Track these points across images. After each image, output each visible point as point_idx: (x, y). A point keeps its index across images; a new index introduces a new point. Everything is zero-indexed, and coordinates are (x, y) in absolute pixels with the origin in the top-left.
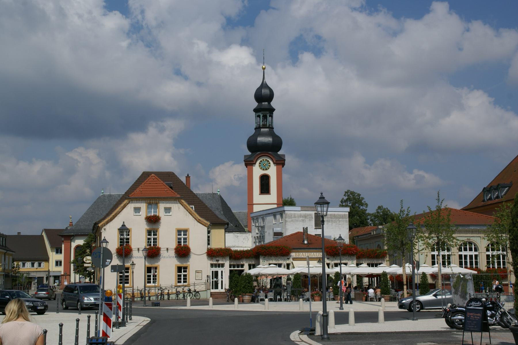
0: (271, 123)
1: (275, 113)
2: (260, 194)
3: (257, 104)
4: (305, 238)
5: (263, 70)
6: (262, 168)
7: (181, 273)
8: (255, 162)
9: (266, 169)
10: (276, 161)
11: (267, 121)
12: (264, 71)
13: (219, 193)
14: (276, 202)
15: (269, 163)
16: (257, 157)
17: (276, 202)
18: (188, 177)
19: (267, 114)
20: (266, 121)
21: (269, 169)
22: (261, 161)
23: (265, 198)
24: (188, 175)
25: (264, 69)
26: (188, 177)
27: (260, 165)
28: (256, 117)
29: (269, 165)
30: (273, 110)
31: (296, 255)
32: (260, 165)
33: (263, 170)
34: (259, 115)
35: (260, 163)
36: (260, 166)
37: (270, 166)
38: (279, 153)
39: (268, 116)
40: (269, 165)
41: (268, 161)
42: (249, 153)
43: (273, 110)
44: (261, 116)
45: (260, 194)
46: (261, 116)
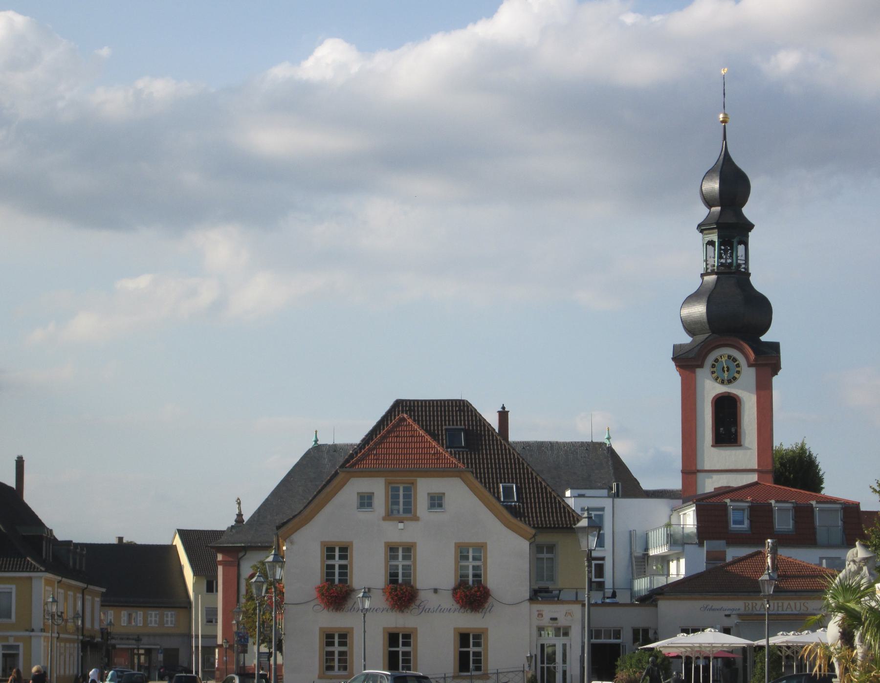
2: (713, 446)
6: (718, 377)
7: (398, 646)
8: (699, 363)
9: (730, 382)
14: (756, 467)
15: (738, 366)
17: (756, 467)
18: (503, 415)
22: (716, 360)
23: (727, 457)
24: (503, 408)
26: (503, 415)
28: (705, 245)
29: (738, 369)
30: (750, 227)
31: (747, 608)
32: (715, 369)
33: (723, 382)
34: (712, 241)
35: (713, 366)
36: (713, 373)
37: (738, 372)
38: (763, 338)
40: (738, 369)
41: (735, 360)
43: (750, 226)
45: (713, 446)
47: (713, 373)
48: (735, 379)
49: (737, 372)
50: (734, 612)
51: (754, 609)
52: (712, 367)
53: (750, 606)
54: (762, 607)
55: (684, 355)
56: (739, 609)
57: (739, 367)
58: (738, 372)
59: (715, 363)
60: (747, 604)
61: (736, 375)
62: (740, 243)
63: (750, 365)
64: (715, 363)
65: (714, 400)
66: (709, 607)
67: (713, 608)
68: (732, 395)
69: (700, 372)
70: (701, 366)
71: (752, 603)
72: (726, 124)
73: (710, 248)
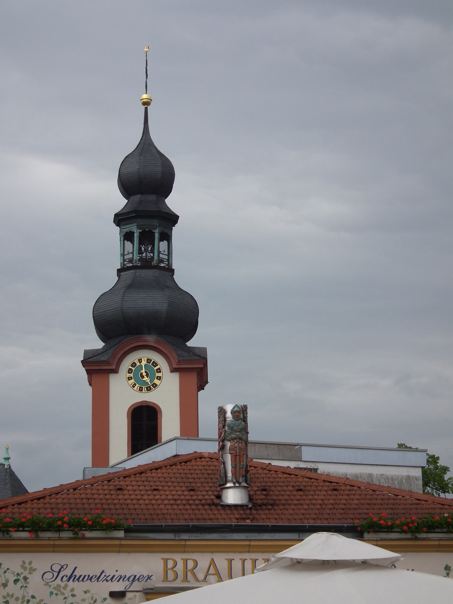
0: (166, 257)
1: (176, 231)
3: (127, 201)
4: (230, 474)
5: (143, 107)
6: (135, 384)
8: (113, 367)
9: (149, 389)
10: (179, 362)
11: (152, 251)
12: (146, 109)
13: (6, 463)
15: (159, 371)
16: (122, 352)
19: (155, 229)
20: (151, 250)
21: (158, 389)
22: (134, 365)
25: (146, 104)
27: (131, 375)
28: (122, 239)
29: (158, 375)
31: (171, 575)
32: (131, 375)
34: (130, 231)
35: (130, 371)
38: (190, 344)
39: (157, 236)
40: (158, 375)
41: (155, 364)
42: (99, 344)
44: (136, 235)
46: (136, 235)
47: (130, 378)
48: (155, 385)
49: (157, 378)
50: (137, 586)
51: (189, 573)
52: (129, 373)
53: (180, 566)
54: (212, 571)
55: (94, 358)
56: (149, 577)
57: (160, 372)
58: (159, 378)
59: (132, 368)
60: (170, 564)
61: (156, 381)
62: (161, 239)
63: (173, 370)
64: (132, 368)
65: (130, 413)
66: (68, 572)
67: (77, 573)
68: (151, 405)
69: (113, 379)
70: (115, 371)
71: (186, 561)
72: (148, 107)
73: (128, 244)
